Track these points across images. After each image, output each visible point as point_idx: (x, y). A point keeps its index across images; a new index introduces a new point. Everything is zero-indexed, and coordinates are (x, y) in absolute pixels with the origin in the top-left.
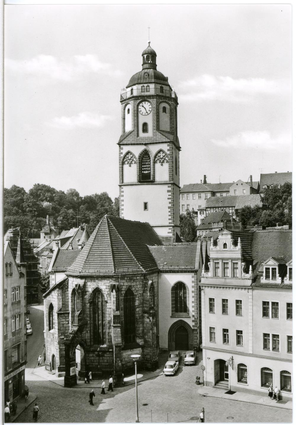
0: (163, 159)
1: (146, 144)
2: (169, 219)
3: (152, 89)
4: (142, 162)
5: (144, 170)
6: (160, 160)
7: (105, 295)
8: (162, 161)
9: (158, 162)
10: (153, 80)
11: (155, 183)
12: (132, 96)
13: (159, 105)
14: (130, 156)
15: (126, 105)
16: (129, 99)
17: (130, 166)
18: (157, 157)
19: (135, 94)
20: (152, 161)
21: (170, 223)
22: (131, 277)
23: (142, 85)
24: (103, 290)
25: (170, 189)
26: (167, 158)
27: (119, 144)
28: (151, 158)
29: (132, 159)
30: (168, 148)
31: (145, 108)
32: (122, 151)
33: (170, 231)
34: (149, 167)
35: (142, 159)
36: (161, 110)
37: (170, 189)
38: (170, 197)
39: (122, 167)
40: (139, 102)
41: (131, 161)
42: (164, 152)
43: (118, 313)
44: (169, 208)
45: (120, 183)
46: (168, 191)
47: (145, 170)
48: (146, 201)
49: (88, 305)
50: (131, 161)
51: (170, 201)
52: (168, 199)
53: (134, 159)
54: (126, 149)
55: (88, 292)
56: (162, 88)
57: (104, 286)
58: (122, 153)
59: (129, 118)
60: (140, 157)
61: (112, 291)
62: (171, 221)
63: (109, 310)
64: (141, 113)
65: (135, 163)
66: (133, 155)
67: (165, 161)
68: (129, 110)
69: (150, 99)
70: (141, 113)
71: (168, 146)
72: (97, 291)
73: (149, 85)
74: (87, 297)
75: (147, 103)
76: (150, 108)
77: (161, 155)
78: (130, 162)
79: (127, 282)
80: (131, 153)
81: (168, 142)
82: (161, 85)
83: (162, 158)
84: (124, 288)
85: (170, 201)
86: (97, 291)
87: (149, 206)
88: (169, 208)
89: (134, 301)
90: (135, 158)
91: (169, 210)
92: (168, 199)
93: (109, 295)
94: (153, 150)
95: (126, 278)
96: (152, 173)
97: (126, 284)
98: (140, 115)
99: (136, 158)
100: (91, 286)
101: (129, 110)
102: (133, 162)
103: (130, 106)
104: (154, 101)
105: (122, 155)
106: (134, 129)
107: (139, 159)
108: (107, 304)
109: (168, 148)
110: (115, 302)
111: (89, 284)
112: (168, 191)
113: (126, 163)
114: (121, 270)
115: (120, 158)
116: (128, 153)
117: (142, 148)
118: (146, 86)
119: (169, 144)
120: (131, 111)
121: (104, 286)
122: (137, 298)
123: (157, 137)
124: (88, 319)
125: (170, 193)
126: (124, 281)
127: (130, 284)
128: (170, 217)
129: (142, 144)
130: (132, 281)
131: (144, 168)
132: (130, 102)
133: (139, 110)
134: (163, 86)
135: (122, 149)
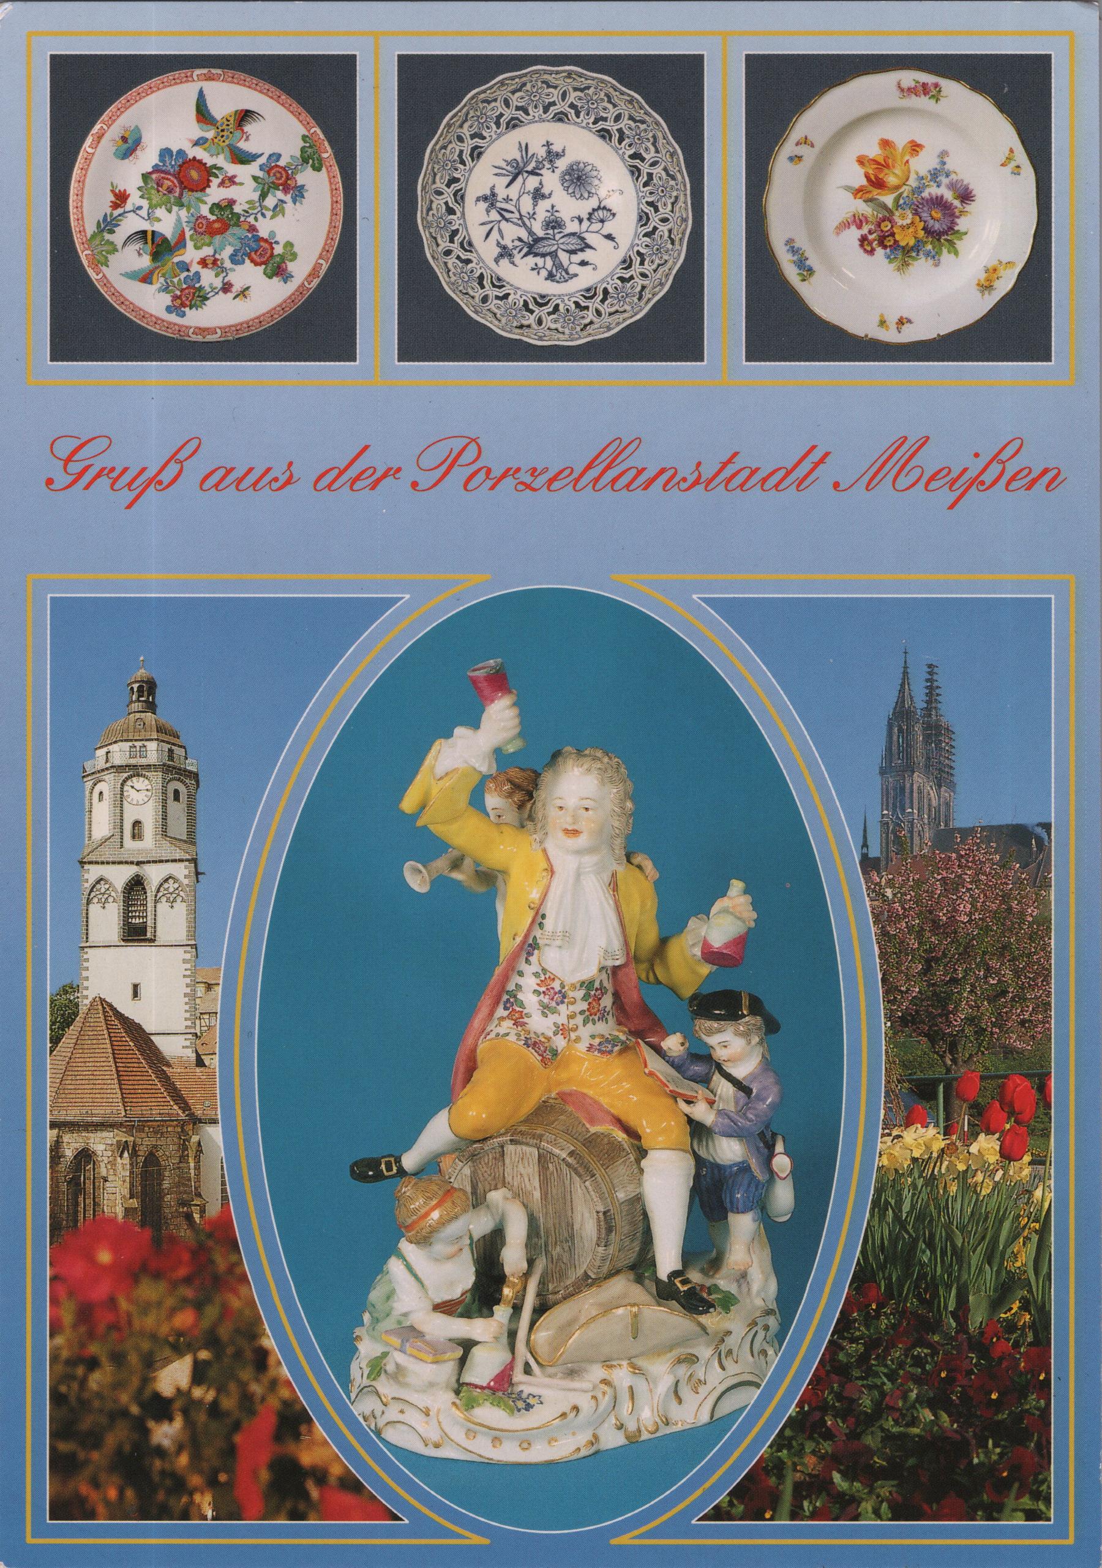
1: (138, 863)
2: (186, 1019)
3: (153, 752)
5: (132, 917)
7: (103, 1165)
9: (164, 899)
10: (155, 735)
11: (156, 943)
12: (108, 765)
14: (103, 887)
16: (103, 770)
19: (118, 759)
21: (187, 1027)
22: (158, 1128)
23: (130, 744)
24: (99, 1153)
25: (188, 956)
26: (182, 893)
28: (148, 891)
30: (186, 872)
33: (188, 1043)
36: (171, 795)
37: (188, 956)
38: (188, 973)
42: (176, 880)
43: (134, 1203)
44: (186, 995)
46: (185, 961)
47: (135, 917)
48: (136, 982)
49: (64, 1187)
51: (188, 980)
52: (184, 976)
53: (113, 894)
55: (64, 1157)
56: (171, 751)
57: (101, 1143)
61: (121, 1156)
62: (189, 1023)
63: (112, 1197)
71: (186, 867)
72: (85, 1156)
73: (146, 743)
74: (62, 1167)
75: (141, 779)
77: (171, 886)
80: (107, 882)
81: (187, 860)
84: (143, 1151)
85: (188, 980)
86: (85, 1156)
87: (143, 991)
88: (186, 995)
89: (160, 1177)
91: (186, 1000)
92: (184, 976)
93: (113, 1164)
94: (154, 875)
96: (150, 923)
99: (116, 891)
100: (72, 1145)
101: (101, 793)
102: (111, 900)
108: (107, 1184)
110: (128, 1179)
111: (67, 1138)
112: (185, 961)
114: (137, 1111)
117: (132, 870)
120: (106, 795)
121: (101, 1143)
122: (167, 1173)
124: (64, 1216)
125: (188, 966)
126: (144, 1135)
128: (188, 1015)
129: (132, 863)
131: (132, 912)
132: (106, 778)
133: (125, 794)
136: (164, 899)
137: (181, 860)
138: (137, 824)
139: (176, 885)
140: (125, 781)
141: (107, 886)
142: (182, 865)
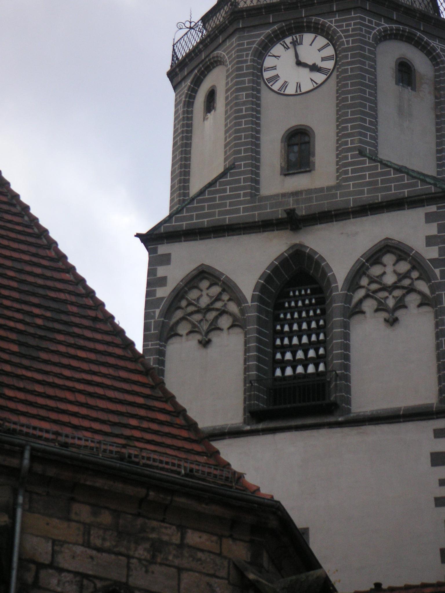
1: (293, 222)
4: (277, 319)
8: (391, 303)
9: (369, 305)
15: (197, 82)
17: (205, 343)
18: (364, 281)
27: (149, 239)
29: (219, 305)
30: (433, 229)
31: (299, 63)
32: (161, 271)
34: (316, 346)
35: (279, 307)
40: (268, 36)
41: (211, 315)
50: (211, 315)
54: (187, 258)
58: (162, 281)
64: (276, 87)
65: (232, 326)
66: (229, 288)
67: (413, 299)
68: (211, 96)
69: (331, 13)
70: (276, 87)
71: (429, 218)
78: (205, 327)
79: (87, 544)
90: (236, 296)
94: (339, 248)
95: (83, 512)
97: (76, 558)
98: (267, 98)
103: (217, 79)
105: (164, 292)
107: (261, 300)
109: (433, 229)
113: (183, 329)
116: (203, 274)
119: (433, 208)
123: (369, 184)
126: (59, 528)
127: (117, 574)
130: (141, 552)
131: (283, 349)
133: (267, 75)
135: (166, 260)
139: (404, 267)
141: (216, 290)
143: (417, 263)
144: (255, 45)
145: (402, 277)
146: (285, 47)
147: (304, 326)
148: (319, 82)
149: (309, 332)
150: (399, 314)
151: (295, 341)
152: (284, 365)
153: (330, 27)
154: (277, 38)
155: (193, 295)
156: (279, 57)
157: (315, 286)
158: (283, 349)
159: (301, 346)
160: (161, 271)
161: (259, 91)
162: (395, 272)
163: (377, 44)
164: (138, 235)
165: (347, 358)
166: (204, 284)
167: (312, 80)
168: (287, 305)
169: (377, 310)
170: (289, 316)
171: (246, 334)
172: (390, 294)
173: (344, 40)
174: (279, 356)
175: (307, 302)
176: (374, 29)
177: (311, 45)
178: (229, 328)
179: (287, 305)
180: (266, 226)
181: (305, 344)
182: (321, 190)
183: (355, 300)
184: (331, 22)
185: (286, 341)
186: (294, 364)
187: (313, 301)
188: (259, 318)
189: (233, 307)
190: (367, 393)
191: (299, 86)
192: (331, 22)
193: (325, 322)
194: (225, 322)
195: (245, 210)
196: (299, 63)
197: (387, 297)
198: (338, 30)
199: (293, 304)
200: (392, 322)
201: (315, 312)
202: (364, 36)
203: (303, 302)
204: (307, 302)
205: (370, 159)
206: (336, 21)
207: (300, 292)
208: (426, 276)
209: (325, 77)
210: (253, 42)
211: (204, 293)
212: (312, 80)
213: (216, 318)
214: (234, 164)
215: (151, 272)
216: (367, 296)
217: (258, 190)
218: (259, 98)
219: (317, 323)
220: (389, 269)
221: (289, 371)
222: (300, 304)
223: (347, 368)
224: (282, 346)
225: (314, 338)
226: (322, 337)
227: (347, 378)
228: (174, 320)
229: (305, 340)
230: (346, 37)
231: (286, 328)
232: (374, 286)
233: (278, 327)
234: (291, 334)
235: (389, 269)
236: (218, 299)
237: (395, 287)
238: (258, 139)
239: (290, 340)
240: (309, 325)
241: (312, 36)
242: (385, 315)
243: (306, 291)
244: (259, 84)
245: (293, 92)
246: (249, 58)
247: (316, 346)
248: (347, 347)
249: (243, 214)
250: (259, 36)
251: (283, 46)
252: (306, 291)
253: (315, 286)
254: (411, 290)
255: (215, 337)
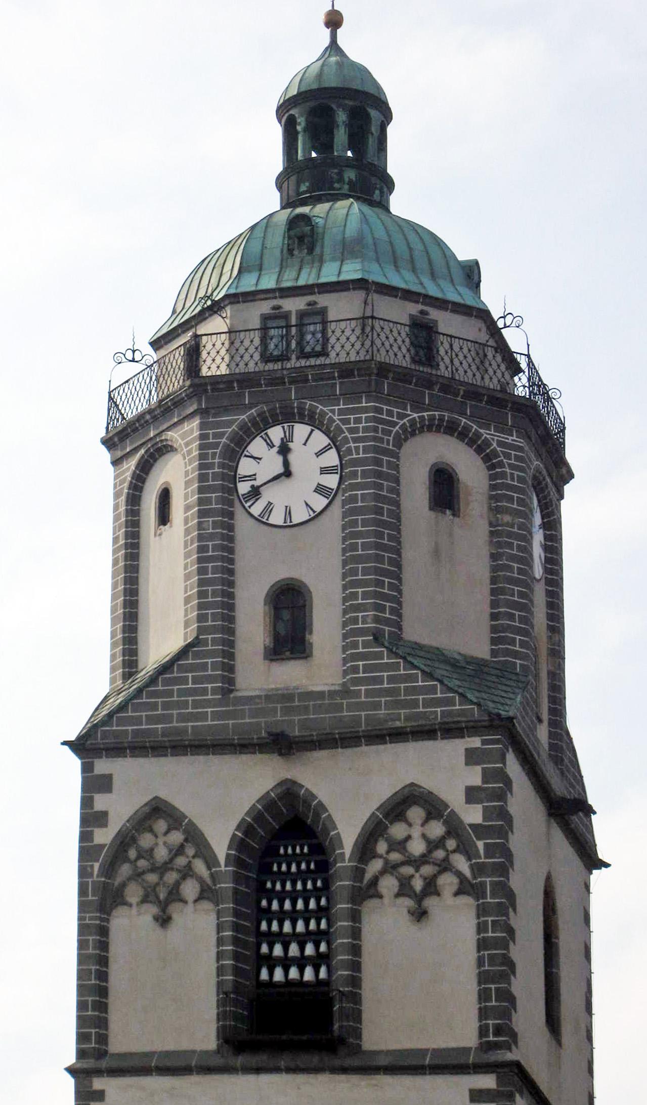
0: (427, 870)
4: (261, 890)
6: (408, 870)
8: (418, 884)
9: (388, 885)
13: (399, 442)
17: (164, 920)
18: (382, 847)
19: (215, 364)
20: (342, 884)
23: (265, 307)
29: (181, 861)
30: (475, 777)
32: (101, 802)
34: (317, 937)
35: (265, 869)
39: (104, 931)
40: (243, 427)
41: (171, 877)
45: (81, 1054)
53: (200, 866)
59: (171, 555)
60: (240, 845)
64: (257, 509)
66: (195, 837)
67: (448, 882)
69: (332, 399)
70: (256, 510)
71: (472, 757)
73: (323, 300)
76: (324, 471)
77: (416, 832)
82: (414, 308)
83: (418, 862)
90: (204, 851)
94: (348, 792)
98: (243, 526)
99: (210, 860)
103: (177, 473)
104: (358, 416)
105: (104, 837)
106: (200, 630)
113: (133, 893)
115: (87, 852)
118: (302, 315)
119: (475, 742)
131: (272, 938)
133: (243, 488)
134: (434, 314)
136: (388, 885)
137: (450, 730)
138: (289, 601)
139: (437, 829)
140: (236, 449)
141: (176, 837)
142: (456, 748)
143: (454, 827)
144: (224, 440)
145: (434, 845)
146: (268, 444)
147: (300, 905)
148: (318, 510)
149: (307, 915)
150: (430, 903)
151: (287, 927)
152: (272, 963)
153: (331, 420)
154: (258, 427)
155: (146, 841)
156: (260, 459)
157: (314, 841)
158: (272, 938)
159: (294, 935)
160: (101, 802)
161: (231, 515)
162: (424, 836)
163: (400, 446)
164: (65, 743)
165: (356, 966)
166: (161, 825)
167: (307, 504)
168: (275, 868)
169: (398, 895)
170: (278, 887)
171: (219, 914)
172: (417, 870)
173: (352, 445)
174: (264, 949)
175: (303, 866)
176: (394, 424)
177: (305, 444)
178: (196, 901)
179: (275, 868)
180: (242, 746)
181: (300, 935)
182: (321, 695)
183: (368, 876)
184: (333, 411)
185: (275, 927)
186: (286, 963)
187: (312, 866)
188: (236, 892)
189: (200, 866)
190: (383, 1027)
191: (288, 513)
192: (332, 412)
193: (328, 900)
194: (190, 889)
195: (216, 716)
196: (287, 473)
197: (412, 876)
198: (343, 427)
199: (284, 868)
200: (420, 915)
201: (314, 884)
202: (381, 440)
203: (298, 866)
204: (303, 866)
205: (390, 651)
206: (341, 412)
207: (294, 849)
208: (466, 849)
209: (325, 501)
210: (222, 435)
211: (161, 841)
212: (307, 504)
213: (177, 884)
214: (197, 638)
215: (86, 802)
216: (383, 872)
217: (231, 681)
218: (231, 528)
219: (318, 901)
220: (416, 832)
221: (279, 975)
222: (294, 868)
223: (355, 982)
224: (269, 933)
225: (313, 925)
226: (323, 925)
227: (356, 998)
228: (118, 881)
229: (300, 927)
230: (355, 440)
231: (275, 905)
232: (395, 857)
233: (264, 903)
234: (281, 916)
235: (416, 832)
236: (180, 850)
237: (423, 860)
238: (231, 596)
239: (281, 926)
240: (306, 904)
241: (309, 428)
242: (408, 902)
243: (302, 849)
244: (231, 503)
245: (281, 523)
246: (216, 461)
247: (317, 937)
248: (356, 950)
249: (210, 721)
250: (229, 424)
251: (265, 441)
252: (302, 849)
253: (314, 841)
254: (445, 866)
255: (175, 909)
